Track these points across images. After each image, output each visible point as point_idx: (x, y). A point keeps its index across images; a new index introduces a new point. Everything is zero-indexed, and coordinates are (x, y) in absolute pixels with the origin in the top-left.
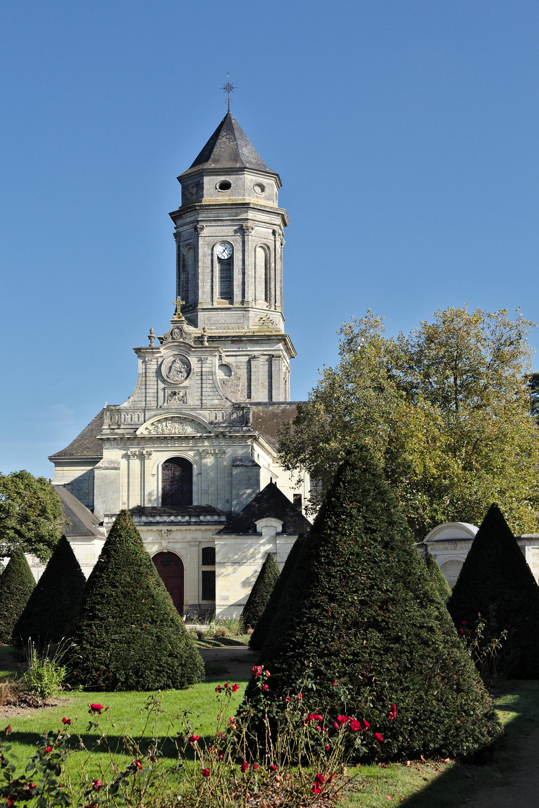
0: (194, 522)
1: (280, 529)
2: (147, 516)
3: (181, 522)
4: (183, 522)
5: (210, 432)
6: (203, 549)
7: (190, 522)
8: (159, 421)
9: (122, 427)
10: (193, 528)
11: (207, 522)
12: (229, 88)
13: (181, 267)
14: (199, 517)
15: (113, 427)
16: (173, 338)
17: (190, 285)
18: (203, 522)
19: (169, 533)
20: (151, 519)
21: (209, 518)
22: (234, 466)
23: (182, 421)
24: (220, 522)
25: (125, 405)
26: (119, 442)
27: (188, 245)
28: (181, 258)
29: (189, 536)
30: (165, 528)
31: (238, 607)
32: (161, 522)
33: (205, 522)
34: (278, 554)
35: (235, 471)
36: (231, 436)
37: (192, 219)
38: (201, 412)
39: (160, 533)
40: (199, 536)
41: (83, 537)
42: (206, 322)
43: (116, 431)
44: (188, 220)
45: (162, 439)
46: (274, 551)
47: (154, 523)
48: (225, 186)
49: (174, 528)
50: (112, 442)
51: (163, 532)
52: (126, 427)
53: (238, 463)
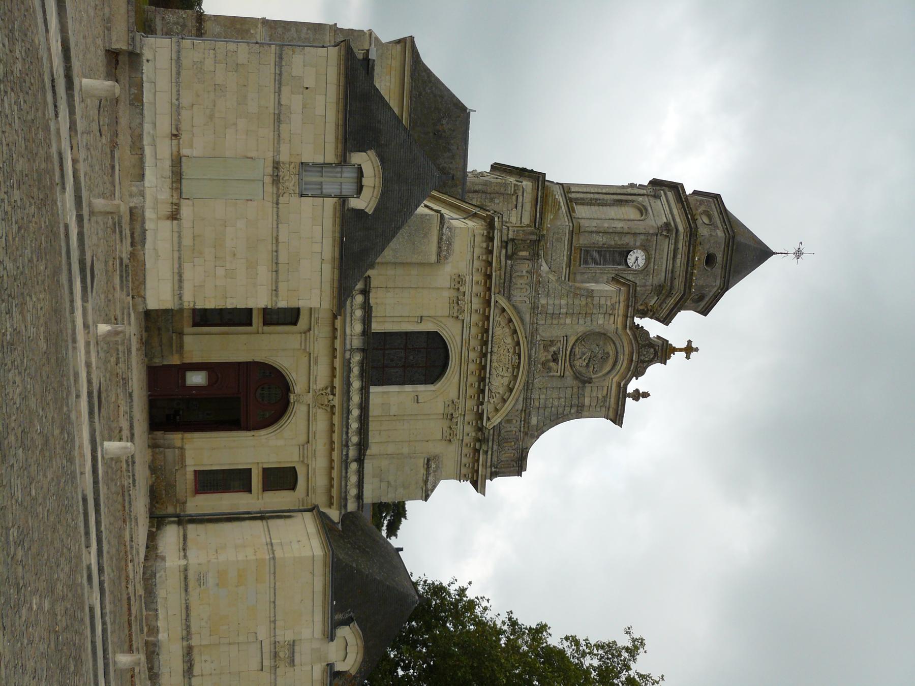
0: (347, 455)
1: (340, 667)
2: (362, 364)
3: (348, 429)
4: (347, 433)
5: (488, 419)
6: (293, 470)
7: (347, 446)
8: (515, 332)
9: (509, 262)
10: (336, 455)
11: (346, 477)
12: (799, 254)
13: (619, 197)
14: (355, 460)
15: (510, 247)
16: (644, 346)
17: (597, 208)
18: (347, 468)
19: (329, 409)
20: (356, 370)
21: (353, 479)
22: (428, 460)
23: (510, 370)
24: (346, 499)
25: (545, 267)
26: (484, 257)
27: (646, 210)
28: (630, 198)
29: (320, 445)
30: (336, 401)
31: (184, 606)
32: (348, 392)
33: (346, 473)
34: (292, 669)
35: (421, 462)
36: (478, 451)
37: (678, 220)
38: (521, 399)
39: (329, 390)
40: (319, 464)
41: (336, 284)
42: (556, 236)
43: (504, 252)
44: (675, 212)
45: (482, 336)
46: (297, 661)
47: (349, 377)
48: (710, 260)
49: (336, 419)
50: (484, 245)
51: (331, 397)
52: (509, 268)
53: (433, 466)
